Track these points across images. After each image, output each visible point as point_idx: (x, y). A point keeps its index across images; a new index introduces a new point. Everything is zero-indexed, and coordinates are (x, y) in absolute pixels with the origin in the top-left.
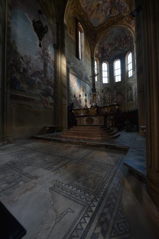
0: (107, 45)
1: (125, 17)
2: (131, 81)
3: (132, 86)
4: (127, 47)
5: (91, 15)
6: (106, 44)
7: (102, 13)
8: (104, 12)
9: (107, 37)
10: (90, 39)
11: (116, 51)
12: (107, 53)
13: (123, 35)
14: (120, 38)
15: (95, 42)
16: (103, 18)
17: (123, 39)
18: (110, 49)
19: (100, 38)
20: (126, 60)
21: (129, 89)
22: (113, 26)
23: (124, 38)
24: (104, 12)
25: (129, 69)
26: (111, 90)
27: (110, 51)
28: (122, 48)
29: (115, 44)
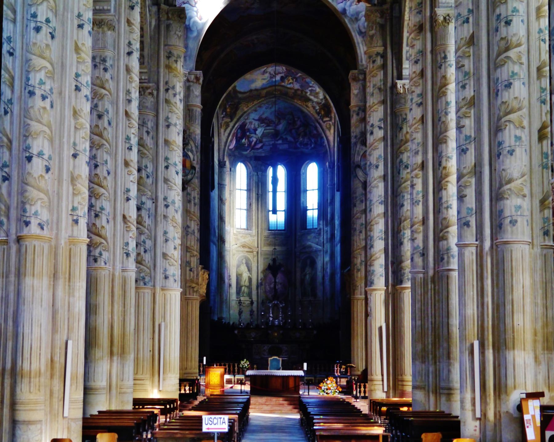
0: (256, 120)
1: (313, 102)
2: (313, 243)
3: (317, 258)
4: (307, 144)
6: (254, 119)
8: (267, 75)
9: (260, 107)
10: (222, 114)
11: (277, 141)
12: (251, 137)
15: (231, 121)
16: (264, 82)
17: (299, 123)
18: (260, 132)
19: (245, 112)
20: (302, 177)
21: (308, 262)
23: (301, 121)
24: (267, 75)
25: (309, 206)
26: (258, 253)
27: (260, 135)
28: (292, 140)
29: (278, 125)
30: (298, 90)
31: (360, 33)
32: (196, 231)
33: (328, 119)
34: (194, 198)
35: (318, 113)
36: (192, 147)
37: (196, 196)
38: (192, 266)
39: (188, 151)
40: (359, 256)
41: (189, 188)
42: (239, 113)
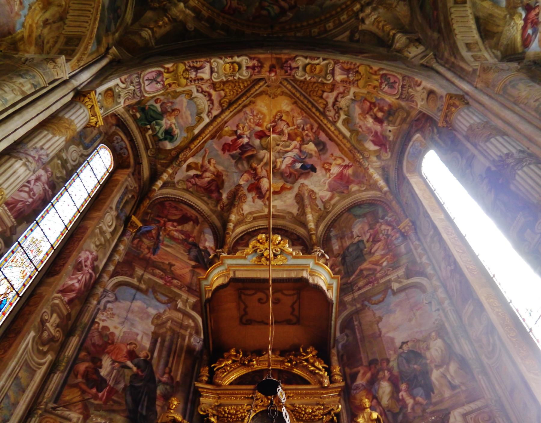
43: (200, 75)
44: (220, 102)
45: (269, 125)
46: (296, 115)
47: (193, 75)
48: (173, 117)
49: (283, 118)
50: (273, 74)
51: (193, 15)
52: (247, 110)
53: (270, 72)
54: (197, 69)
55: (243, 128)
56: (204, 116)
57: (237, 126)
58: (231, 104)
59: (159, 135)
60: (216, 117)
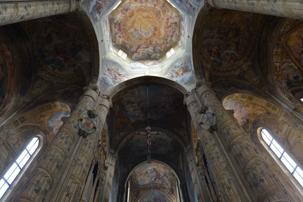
5: (139, 176)
7: (148, 177)
8: (149, 177)
9: (147, 195)
13: (163, 199)
14: (159, 200)
15: (137, 198)
16: (149, 181)
19: (142, 195)
22: (155, 190)
24: (149, 177)
30: (161, 184)
31: (186, 84)
32: (85, 165)
33: (173, 195)
34: (90, 143)
35: (169, 194)
36: (97, 119)
37: (92, 143)
38: (71, 191)
39: (94, 120)
40: (225, 176)
41: (88, 138)
42: (140, 195)
43: (278, 67)
44: (286, 59)
45: (301, 40)
46: (300, 30)
47: (278, 69)
48: (290, 76)
49: (300, 35)
50: (282, 40)
51: (246, 63)
52: (291, 49)
53: (281, 41)
54: (276, 68)
55: (298, 50)
56: (291, 65)
57: (297, 53)
58: (288, 55)
59: (295, 81)
60: (292, 60)
